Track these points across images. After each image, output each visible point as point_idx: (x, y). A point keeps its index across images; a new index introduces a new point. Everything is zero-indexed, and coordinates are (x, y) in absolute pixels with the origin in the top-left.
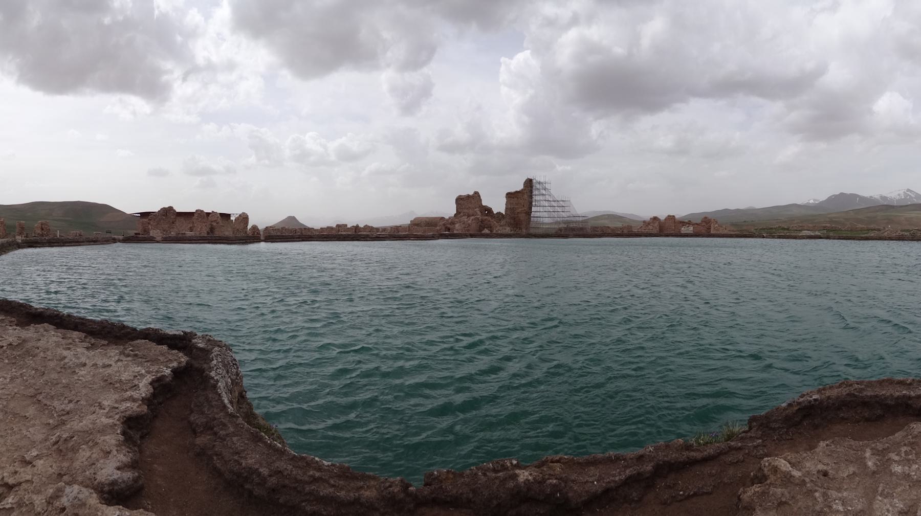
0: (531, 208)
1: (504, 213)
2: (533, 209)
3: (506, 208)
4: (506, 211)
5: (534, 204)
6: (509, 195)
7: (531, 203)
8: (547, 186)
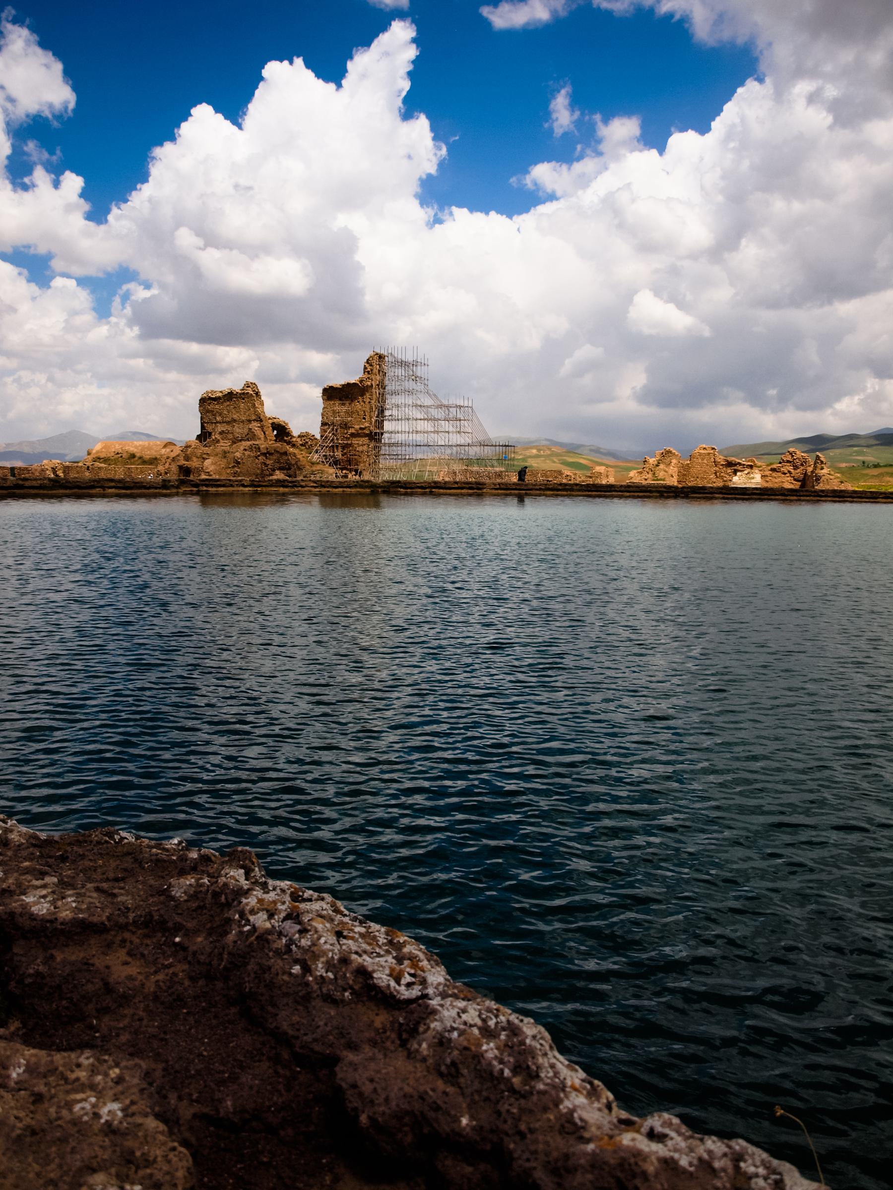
0: (380, 425)
1: (318, 436)
2: (387, 426)
3: (324, 424)
4: (323, 431)
5: (387, 413)
6: (330, 393)
7: (382, 411)
8: (419, 371)
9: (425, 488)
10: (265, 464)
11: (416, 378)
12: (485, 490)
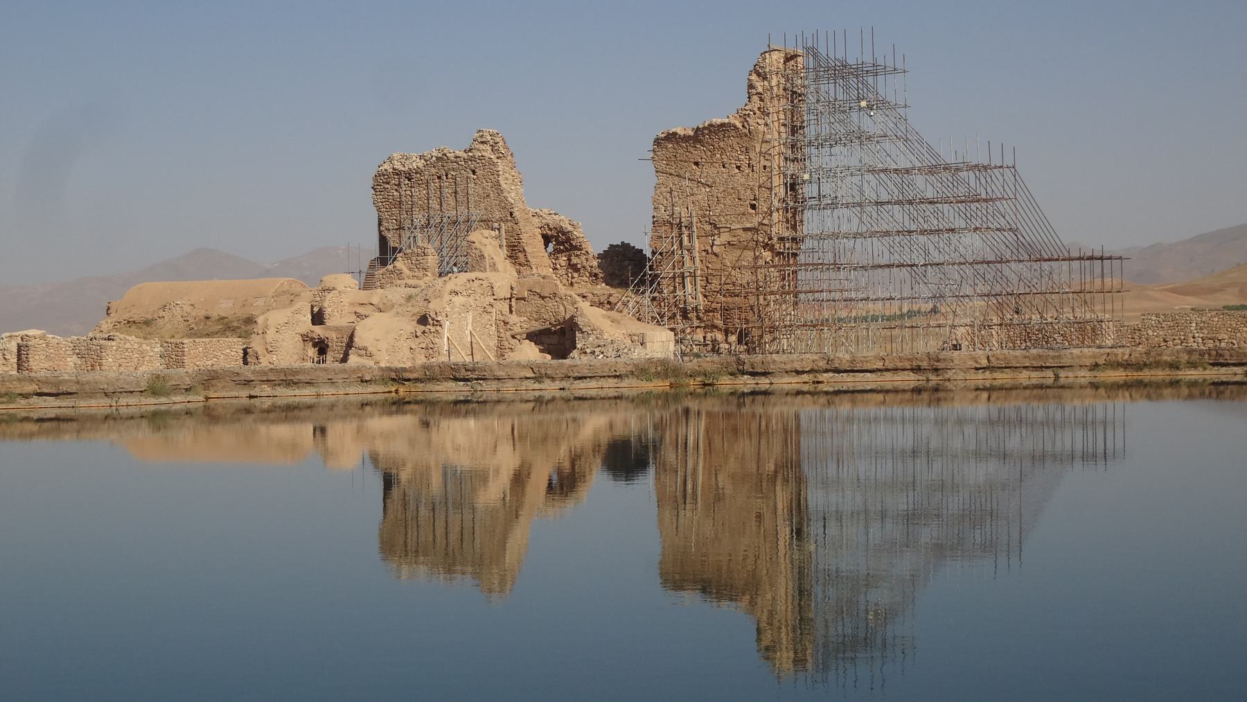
0: (793, 218)
2: (812, 222)
5: (808, 191)
8: (887, 87)
9: (803, 372)
10: (506, 323)
11: (880, 104)
12: (950, 374)
